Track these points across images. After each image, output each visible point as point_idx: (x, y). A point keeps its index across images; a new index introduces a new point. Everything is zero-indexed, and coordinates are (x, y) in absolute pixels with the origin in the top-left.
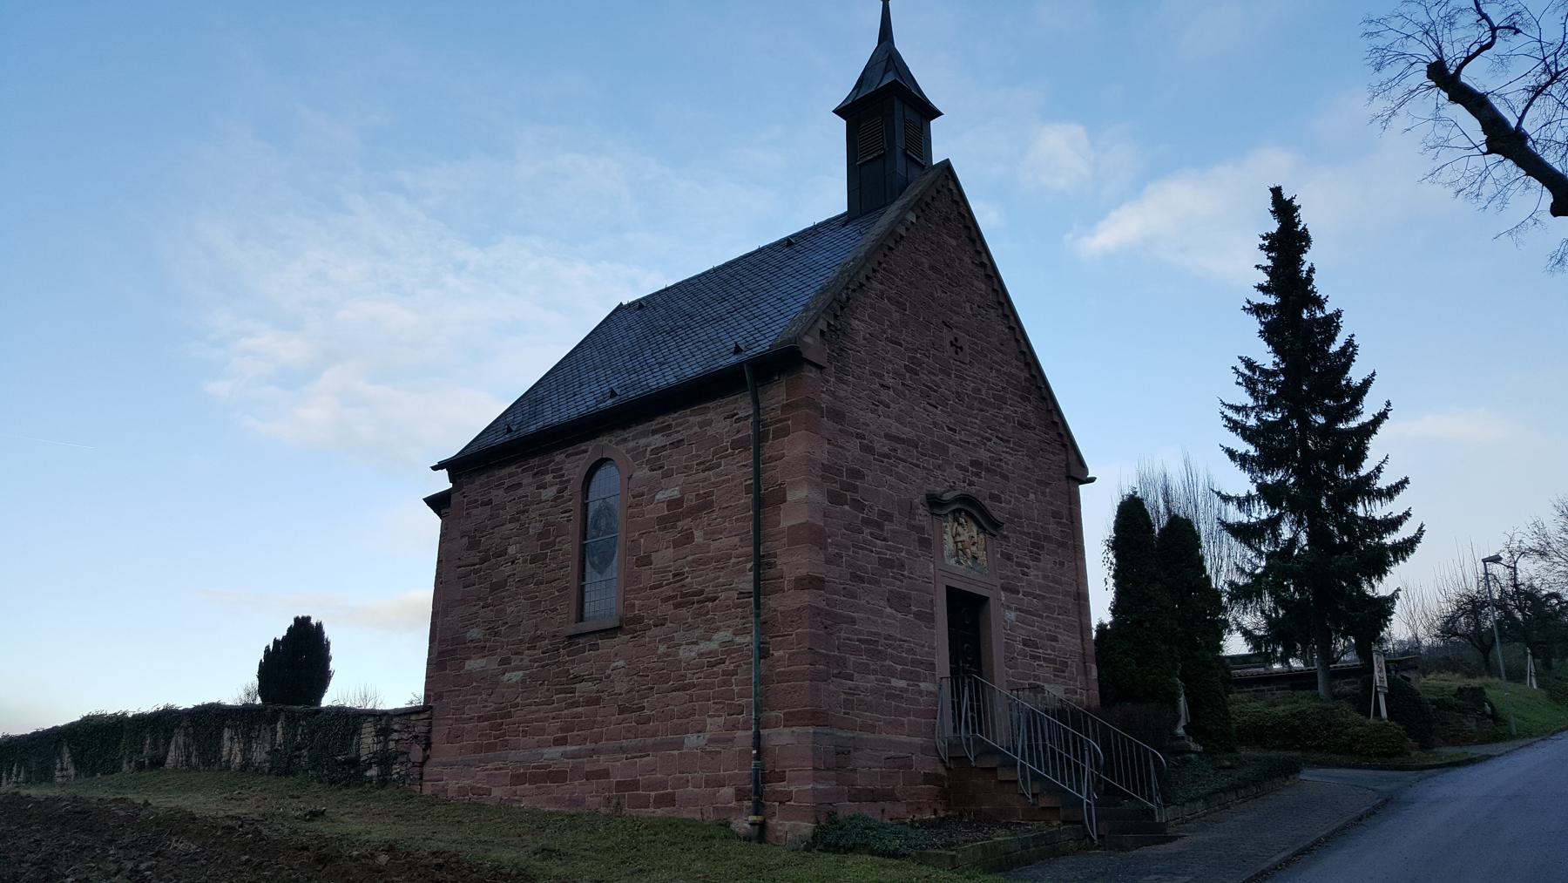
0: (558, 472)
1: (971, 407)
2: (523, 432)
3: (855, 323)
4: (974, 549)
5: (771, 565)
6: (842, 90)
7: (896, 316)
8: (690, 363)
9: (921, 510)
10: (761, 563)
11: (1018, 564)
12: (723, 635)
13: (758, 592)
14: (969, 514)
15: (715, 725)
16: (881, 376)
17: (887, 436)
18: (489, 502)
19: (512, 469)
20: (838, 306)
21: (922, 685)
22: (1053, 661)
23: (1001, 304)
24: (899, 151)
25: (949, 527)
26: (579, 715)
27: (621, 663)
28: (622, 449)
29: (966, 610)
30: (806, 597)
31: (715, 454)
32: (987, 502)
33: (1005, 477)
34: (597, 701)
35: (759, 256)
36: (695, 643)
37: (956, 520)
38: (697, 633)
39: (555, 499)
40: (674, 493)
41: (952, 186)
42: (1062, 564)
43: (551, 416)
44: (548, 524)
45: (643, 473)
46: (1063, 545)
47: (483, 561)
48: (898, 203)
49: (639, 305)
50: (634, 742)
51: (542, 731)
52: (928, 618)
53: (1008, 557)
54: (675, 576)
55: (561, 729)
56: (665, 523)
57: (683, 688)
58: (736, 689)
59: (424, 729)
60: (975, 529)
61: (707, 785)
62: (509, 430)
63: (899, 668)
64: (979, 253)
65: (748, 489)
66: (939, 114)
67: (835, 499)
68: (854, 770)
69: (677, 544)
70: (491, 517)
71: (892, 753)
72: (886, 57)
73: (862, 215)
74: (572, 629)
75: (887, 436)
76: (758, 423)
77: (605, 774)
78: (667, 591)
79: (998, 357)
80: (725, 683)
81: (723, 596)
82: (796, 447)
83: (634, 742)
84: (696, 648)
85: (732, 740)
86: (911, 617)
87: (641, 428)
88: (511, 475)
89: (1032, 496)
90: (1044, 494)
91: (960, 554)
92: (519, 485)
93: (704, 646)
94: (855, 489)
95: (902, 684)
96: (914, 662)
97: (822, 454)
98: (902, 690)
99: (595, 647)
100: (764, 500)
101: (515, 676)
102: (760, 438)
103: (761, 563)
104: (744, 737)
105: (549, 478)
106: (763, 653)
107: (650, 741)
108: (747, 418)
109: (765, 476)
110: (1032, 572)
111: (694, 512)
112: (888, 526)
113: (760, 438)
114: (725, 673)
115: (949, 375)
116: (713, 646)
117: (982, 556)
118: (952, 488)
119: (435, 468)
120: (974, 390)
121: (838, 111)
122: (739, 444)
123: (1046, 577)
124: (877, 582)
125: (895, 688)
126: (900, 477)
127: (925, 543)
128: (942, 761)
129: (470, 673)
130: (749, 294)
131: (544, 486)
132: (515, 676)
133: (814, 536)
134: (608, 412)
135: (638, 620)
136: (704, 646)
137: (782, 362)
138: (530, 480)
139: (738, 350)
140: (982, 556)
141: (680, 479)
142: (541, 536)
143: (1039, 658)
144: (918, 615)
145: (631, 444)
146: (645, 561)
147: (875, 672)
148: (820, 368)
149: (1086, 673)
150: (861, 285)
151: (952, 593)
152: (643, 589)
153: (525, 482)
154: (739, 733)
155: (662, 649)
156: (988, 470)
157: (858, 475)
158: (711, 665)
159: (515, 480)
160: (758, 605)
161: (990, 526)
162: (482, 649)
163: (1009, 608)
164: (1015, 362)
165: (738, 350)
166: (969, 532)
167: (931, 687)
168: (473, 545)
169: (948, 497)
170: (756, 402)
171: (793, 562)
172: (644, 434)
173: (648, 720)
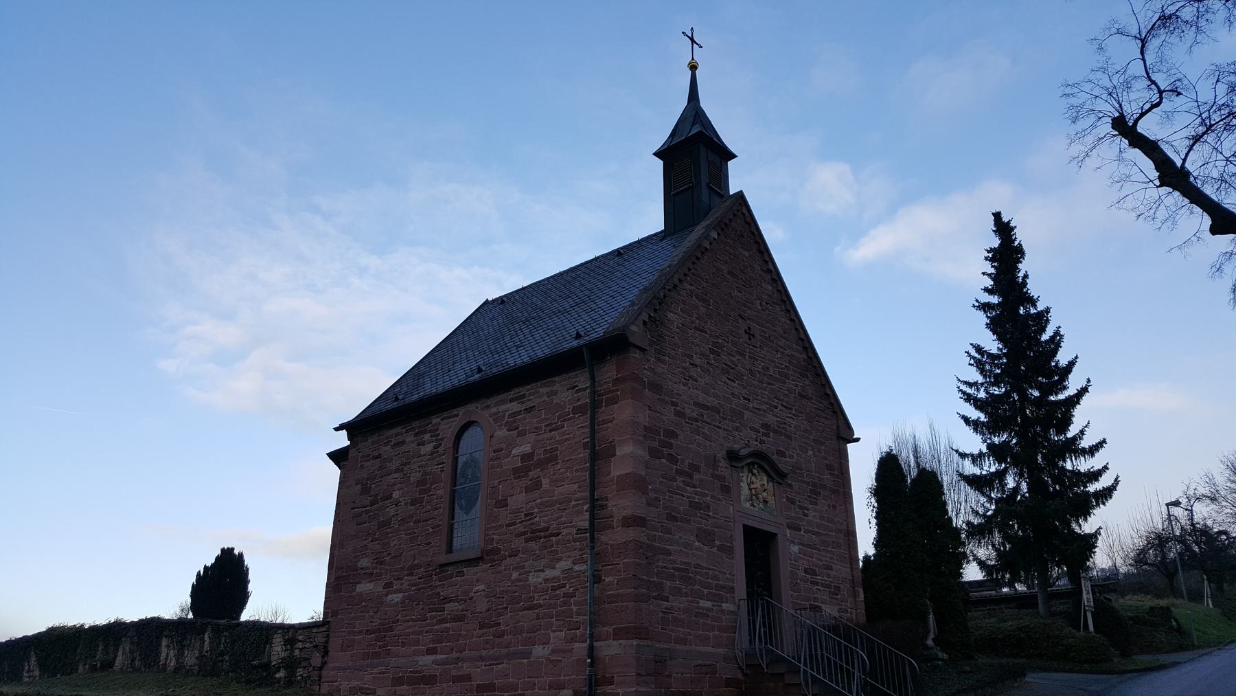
0: (435, 433)
1: (761, 382)
2: (408, 400)
3: (670, 315)
4: (765, 494)
5: (604, 507)
6: (660, 138)
7: (703, 310)
8: (539, 346)
9: (723, 463)
10: (596, 505)
11: (800, 507)
12: (564, 564)
13: (592, 529)
14: (761, 467)
15: (557, 637)
16: (690, 357)
17: (697, 404)
18: (379, 456)
19: (398, 430)
20: (656, 302)
21: (725, 606)
22: (828, 586)
23: (784, 301)
24: (704, 184)
25: (745, 476)
26: (447, 630)
27: (482, 587)
28: (486, 413)
29: (760, 545)
30: (632, 533)
31: (560, 417)
32: (775, 457)
33: (789, 437)
34: (460, 618)
35: (596, 263)
36: (543, 571)
37: (750, 471)
38: (543, 562)
39: (432, 454)
40: (527, 448)
41: (745, 211)
42: (834, 507)
43: (430, 388)
44: (425, 474)
45: (502, 433)
46: (834, 492)
47: (372, 504)
48: (704, 224)
49: (501, 301)
50: (491, 652)
51: (417, 643)
52: (729, 551)
54: (526, 515)
55: (433, 641)
56: (519, 473)
57: (531, 608)
58: (575, 609)
59: (323, 640)
60: (765, 478)
61: (550, 687)
62: (397, 399)
63: (706, 591)
64: (766, 262)
65: (585, 446)
66: (733, 156)
67: (654, 453)
68: (670, 676)
69: (528, 490)
70: (380, 468)
71: (700, 662)
72: (694, 113)
73: (676, 232)
74: (443, 559)
75: (697, 404)
76: (594, 393)
77: (468, 678)
78: (520, 528)
79: (782, 342)
80: (565, 603)
81: (565, 532)
82: (623, 412)
83: (491, 652)
84: (542, 575)
85: (571, 651)
86: (714, 550)
87: (501, 397)
88: (397, 435)
89: (810, 452)
90: (819, 451)
91: (753, 500)
92: (404, 442)
93: (549, 573)
94: (670, 446)
95: (708, 604)
96: (717, 587)
97: (644, 418)
98: (708, 609)
99: (461, 574)
100: (598, 454)
101: (396, 598)
102: (595, 405)
103: (596, 505)
104: (581, 648)
105: (427, 437)
106: (597, 579)
107: (504, 651)
108: (585, 389)
109: (598, 435)
110: (811, 514)
111: (542, 464)
112: (696, 476)
113: (595, 405)
114: (565, 595)
115: (744, 356)
116: (556, 573)
117: (771, 500)
118: (747, 446)
119: (336, 429)
120: (763, 368)
121: (656, 154)
122: (578, 410)
123: (822, 518)
124: (688, 521)
125: (702, 608)
126: (706, 437)
127: (726, 490)
128: (740, 668)
129: (360, 594)
130: (587, 292)
131: (423, 444)
132: (396, 598)
133: (637, 483)
134: (558, 372)
135: (496, 551)
136: (549, 573)
137: (614, 345)
138: (412, 438)
139: (578, 336)
140: (771, 500)
141: (532, 437)
142: (421, 482)
143: (817, 584)
144: (720, 548)
145: (494, 410)
146: (503, 503)
147: (686, 595)
148: (643, 350)
149: (855, 595)
150: (675, 286)
151: (748, 530)
152: (501, 526)
153: (407, 440)
154: (577, 645)
155: (515, 575)
156: (775, 431)
157: (672, 434)
158: (554, 589)
159: (400, 438)
160: (592, 538)
161: (777, 475)
162: (370, 576)
163: (793, 542)
164: (795, 346)
165: (578, 336)
166: (761, 481)
167: (732, 608)
168: (365, 491)
169: (744, 452)
170: (593, 378)
171: (621, 505)
172: (503, 402)
173: (502, 635)
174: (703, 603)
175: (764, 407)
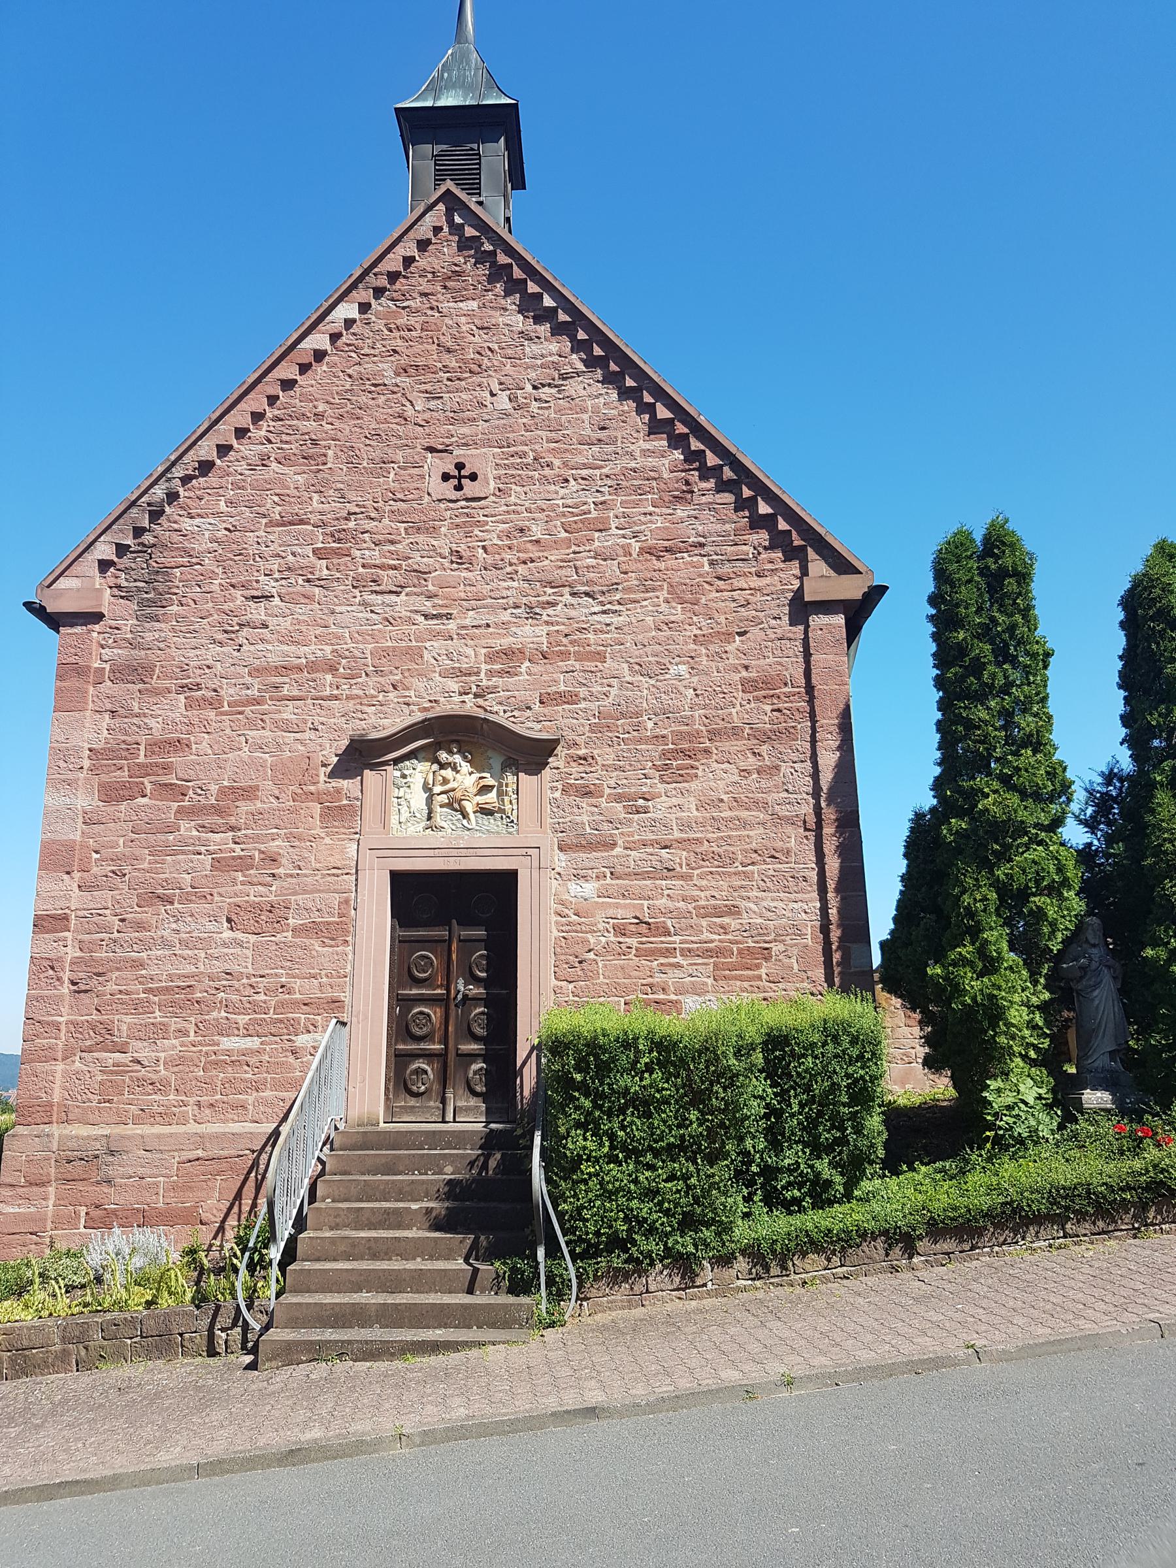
11: (619, 798)
17: (255, 672)
52: (337, 931)
53: (587, 793)
63: (242, 1019)
67: (111, 794)
75: (255, 672)
95: (254, 1043)
125: (228, 1053)
143: (670, 952)
174: (227, 1043)
175: (506, 616)
